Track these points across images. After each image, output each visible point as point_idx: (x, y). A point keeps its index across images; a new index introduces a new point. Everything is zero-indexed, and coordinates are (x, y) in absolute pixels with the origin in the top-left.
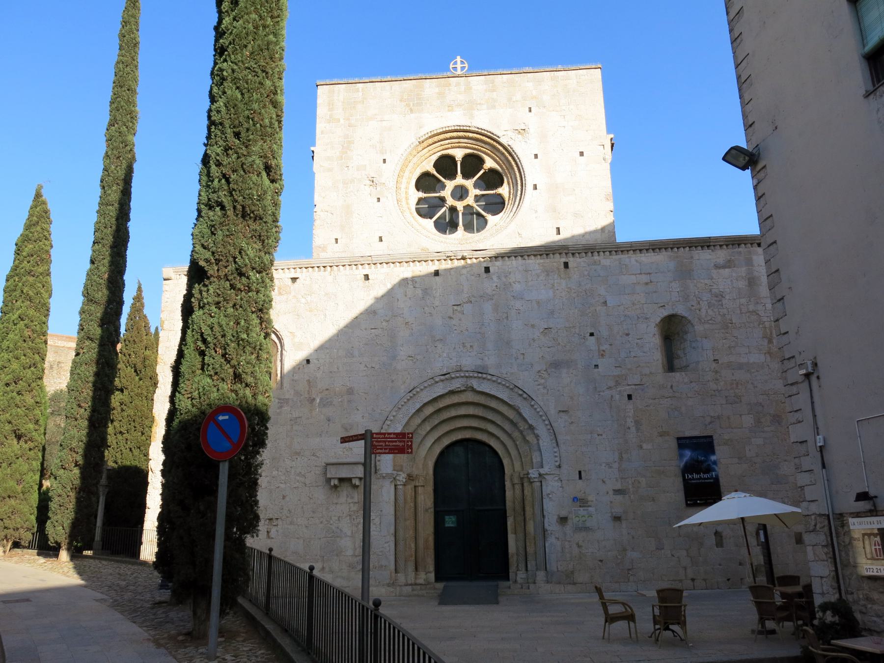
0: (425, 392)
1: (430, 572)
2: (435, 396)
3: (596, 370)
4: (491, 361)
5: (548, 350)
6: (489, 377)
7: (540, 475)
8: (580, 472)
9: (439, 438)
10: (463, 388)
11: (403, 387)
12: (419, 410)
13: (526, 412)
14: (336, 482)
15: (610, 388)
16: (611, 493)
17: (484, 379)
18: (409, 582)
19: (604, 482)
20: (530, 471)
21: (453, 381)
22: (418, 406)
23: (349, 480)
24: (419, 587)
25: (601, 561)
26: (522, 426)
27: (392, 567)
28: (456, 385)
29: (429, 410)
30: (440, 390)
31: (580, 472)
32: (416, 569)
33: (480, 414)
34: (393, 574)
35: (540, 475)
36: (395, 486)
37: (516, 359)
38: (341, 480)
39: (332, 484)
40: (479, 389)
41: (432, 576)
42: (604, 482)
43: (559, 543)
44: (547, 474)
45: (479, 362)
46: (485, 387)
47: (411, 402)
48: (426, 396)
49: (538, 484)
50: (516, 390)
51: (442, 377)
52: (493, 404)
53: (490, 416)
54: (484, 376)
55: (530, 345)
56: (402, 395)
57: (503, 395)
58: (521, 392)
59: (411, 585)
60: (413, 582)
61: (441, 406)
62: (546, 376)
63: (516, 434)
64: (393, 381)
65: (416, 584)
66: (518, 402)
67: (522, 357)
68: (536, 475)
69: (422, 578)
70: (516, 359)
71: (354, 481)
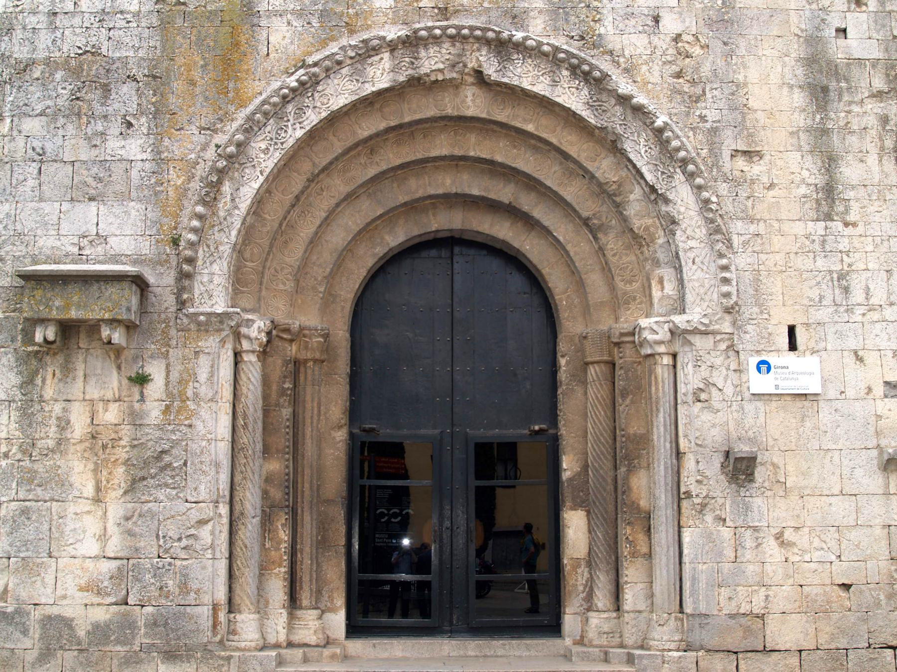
1: (333, 610)
2: (369, 89)
3: (841, 42)
7: (674, 332)
8: (792, 330)
14: (51, 333)
15: (879, 95)
16: (879, 390)
18: (272, 639)
19: (860, 359)
20: (644, 322)
23: (93, 328)
24: (299, 653)
25: (846, 587)
27: (221, 595)
28: (432, 62)
30: (381, 75)
31: (792, 330)
32: (293, 601)
34: (222, 616)
35: (674, 332)
36: (237, 355)
38: (69, 330)
39: (39, 337)
41: (338, 620)
42: (860, 359)
43: (726, 533)
44: (695, 331)
47: (290, 108)
48: (339, 93)
49: (667, 360)
59: (277, 646)
60: (282, 638)
65: (290, 645)
68: (663, 334)
69: (309, 627)
71: (105, 332)
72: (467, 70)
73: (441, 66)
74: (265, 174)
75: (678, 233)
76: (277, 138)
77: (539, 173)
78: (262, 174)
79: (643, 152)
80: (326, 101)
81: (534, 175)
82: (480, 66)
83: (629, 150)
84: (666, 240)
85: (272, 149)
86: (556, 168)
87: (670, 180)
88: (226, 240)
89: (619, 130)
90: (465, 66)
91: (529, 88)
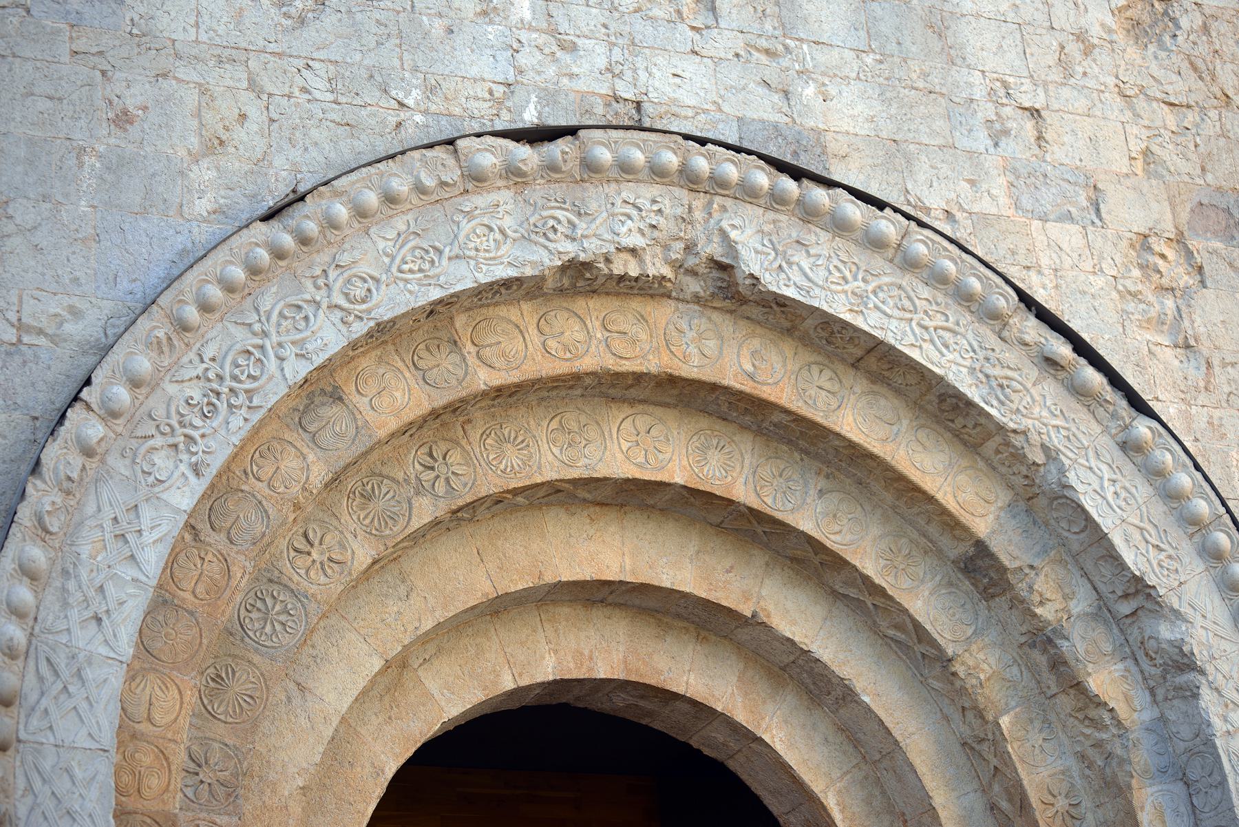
0: (383, 238)
2: (463, 278)
4: (843, 119)
5: (1170, 119)
6: (855, 211)
9: (500, 608)
10: (656, 267)
11: (204, 173)
12: (322, 388)
13: (1104, 489)
17: (809, 214)
21: (595, 196)
22: (329, 337)
26: (1055, 597)
28: (625, 224)
29: (394, 396)
30: (500, 239)
33: (742, 493)
37: (998, 135)
40: (774, 283)
45: (764, 107)
46: (816, 274)
48: (394, 272)
50: (1032, 329)
51: (523, 152)
52: (857, 417)
53: (811, 512)
54: (819, 195)
55: (1064, 63)
56: (203, 234)
57: (950, 352)
58: (1063, 350)
61: (485, 379)
62: (1176, 272)
63: (983, 662)
64: (123, 119)
66: (1037, 410)
67: (1029, 125)
70: (998, 135)
72: (691, 262)
73: (637, 241)
74: (210, 473)
75: (1205, 692)
76: (235, 378)
77: (837, 538)
78: (197, 473)
79: (1110, 498)
80: (359, 292)
81: (828, 544)
82: (735, 254)
83: (1080, 488)
84: (1156, 713)
85: (222, 407)
86: (875, 530)
87: (1175, 565)
88: (104, 650)
89: (1056, 441)
90: (689, 248)
91: (847, 317)
